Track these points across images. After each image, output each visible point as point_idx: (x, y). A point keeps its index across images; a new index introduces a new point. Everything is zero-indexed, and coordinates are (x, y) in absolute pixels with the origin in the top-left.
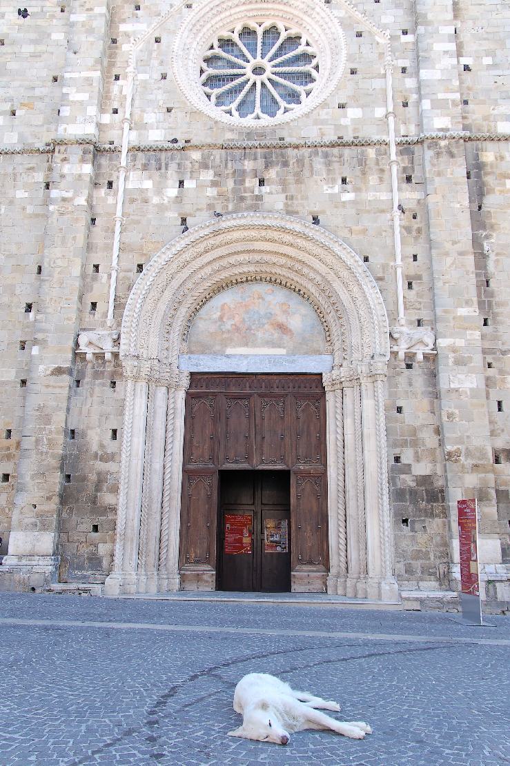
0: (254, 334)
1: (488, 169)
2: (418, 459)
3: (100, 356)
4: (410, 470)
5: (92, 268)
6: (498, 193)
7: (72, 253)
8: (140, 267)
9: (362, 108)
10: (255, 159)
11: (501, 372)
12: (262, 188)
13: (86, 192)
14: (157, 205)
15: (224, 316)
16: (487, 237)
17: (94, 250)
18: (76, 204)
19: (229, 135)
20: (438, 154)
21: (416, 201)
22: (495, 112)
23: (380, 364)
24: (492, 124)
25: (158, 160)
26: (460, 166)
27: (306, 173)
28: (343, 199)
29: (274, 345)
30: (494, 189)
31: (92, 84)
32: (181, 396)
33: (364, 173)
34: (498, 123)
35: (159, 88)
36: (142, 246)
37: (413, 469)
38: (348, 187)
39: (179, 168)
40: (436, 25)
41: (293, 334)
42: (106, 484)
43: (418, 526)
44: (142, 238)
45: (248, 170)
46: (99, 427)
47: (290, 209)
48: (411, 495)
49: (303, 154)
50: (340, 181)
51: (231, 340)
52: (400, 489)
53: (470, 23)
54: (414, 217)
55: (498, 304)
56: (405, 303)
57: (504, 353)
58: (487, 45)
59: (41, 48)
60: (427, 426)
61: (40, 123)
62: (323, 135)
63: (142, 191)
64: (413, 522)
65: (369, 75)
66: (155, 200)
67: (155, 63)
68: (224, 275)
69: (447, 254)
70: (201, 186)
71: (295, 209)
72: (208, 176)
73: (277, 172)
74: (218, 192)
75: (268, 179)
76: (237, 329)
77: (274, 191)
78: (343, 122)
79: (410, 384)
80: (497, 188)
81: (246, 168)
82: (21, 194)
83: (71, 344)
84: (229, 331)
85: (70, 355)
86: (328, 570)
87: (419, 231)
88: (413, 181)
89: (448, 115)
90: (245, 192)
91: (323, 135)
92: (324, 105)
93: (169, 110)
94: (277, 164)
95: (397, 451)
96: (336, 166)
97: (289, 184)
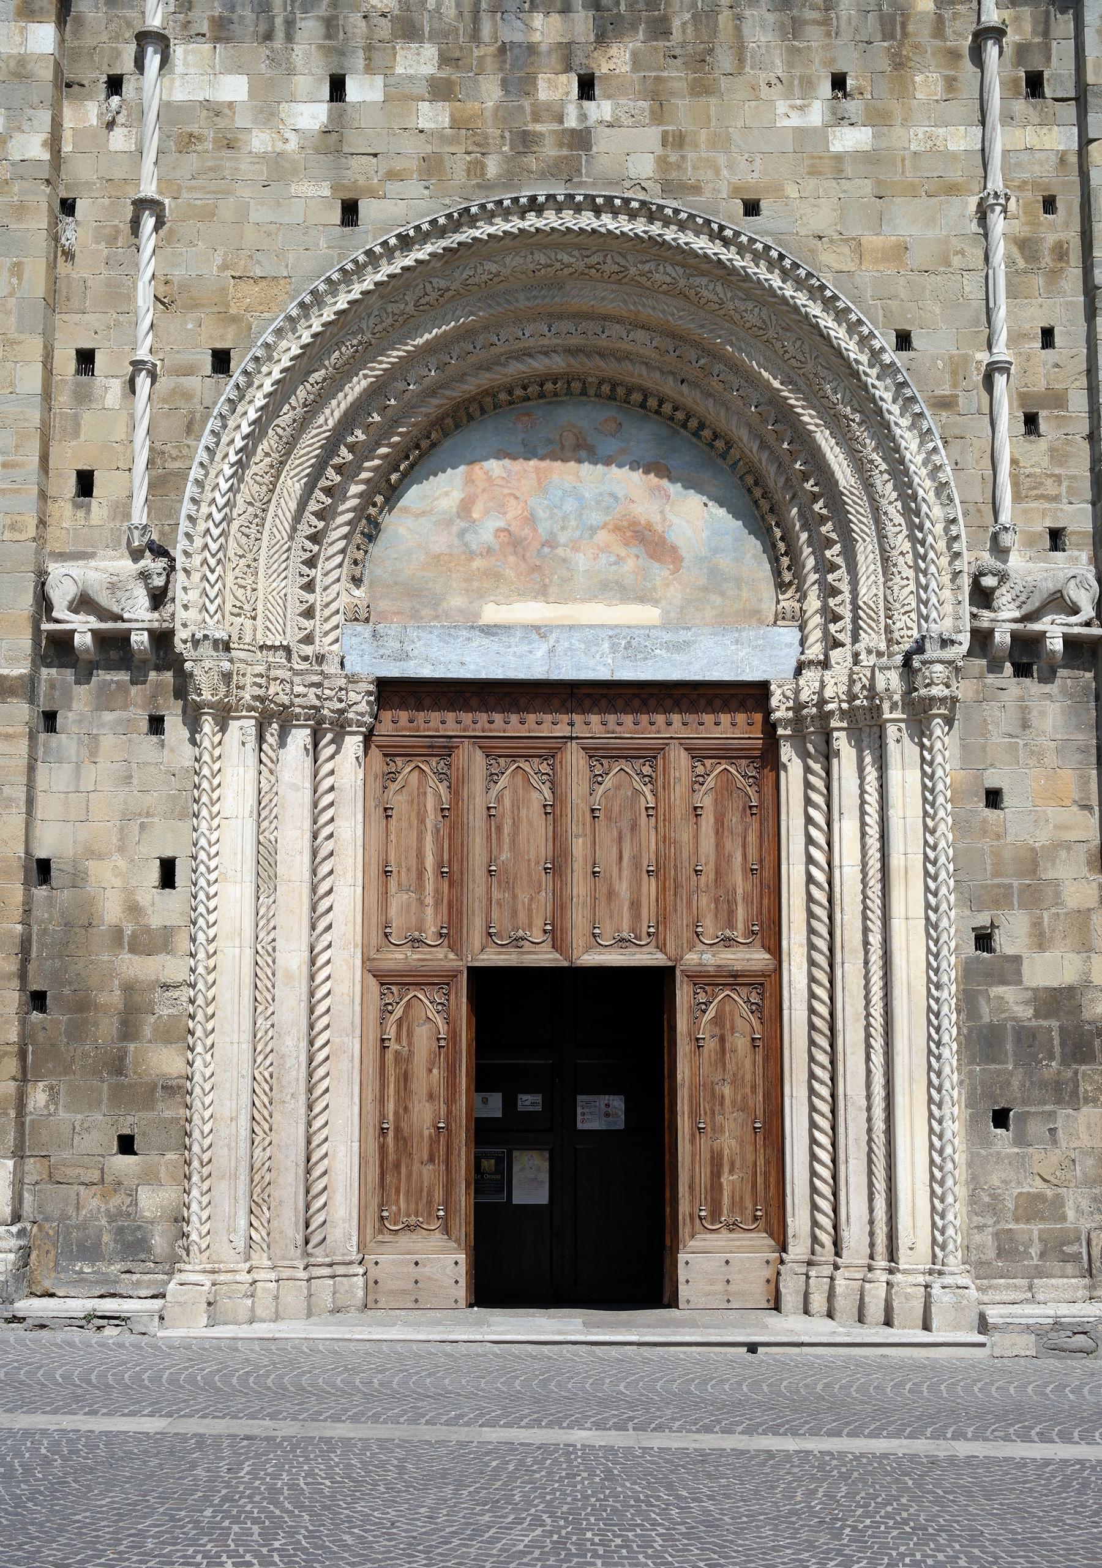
0: (564, 560)
2: (1041, 941)
4: (1019, 973)
5: (66, 362)
7: (13, 319)
8: (221, 361)
13: (45, 117)
14: (263, 157)
15: (473, 503)
17: (75, 303)
18: (17, 157)
21: (1054, 159)
23: (939, 667)
27: (725, 60)
28: (836, 147)
36: (224, 289)
37: (1026, 969)
38: (852, 107)
39: (328, 36)
41: (682, 560)
42: (152, 1019)
43: (1035, 1128)
44: (224, 267)
45: (544, 48)
46: (121, 849)
47: (674, 175)
48: (1018, 1041)
50: (825, 88)
51: (498, 577)
52: (991, 1026)
54: (1049, 205)
56: (1016, 484)
60: (1068, 846)
63: (215, 110)
64: (1023, 1117)
66: (260, 141)
68: (471, 386)
71: (690, 175)
73: (635, 54)
74: (452, 116)
75: (606, 77)
76: (514, 542)
77: (626, 121)
79: (1025, 725)
81: (536, 37)
83: (26, 601)
84: (490, 551)
85: (25, 643)
86: (784, 1248)
87: (1060, 253)
88: (1048, 91)
90: (536, 119)
94: (634, 27)
95: (983, 919)
96: (814, 35)
97: (672, 94)
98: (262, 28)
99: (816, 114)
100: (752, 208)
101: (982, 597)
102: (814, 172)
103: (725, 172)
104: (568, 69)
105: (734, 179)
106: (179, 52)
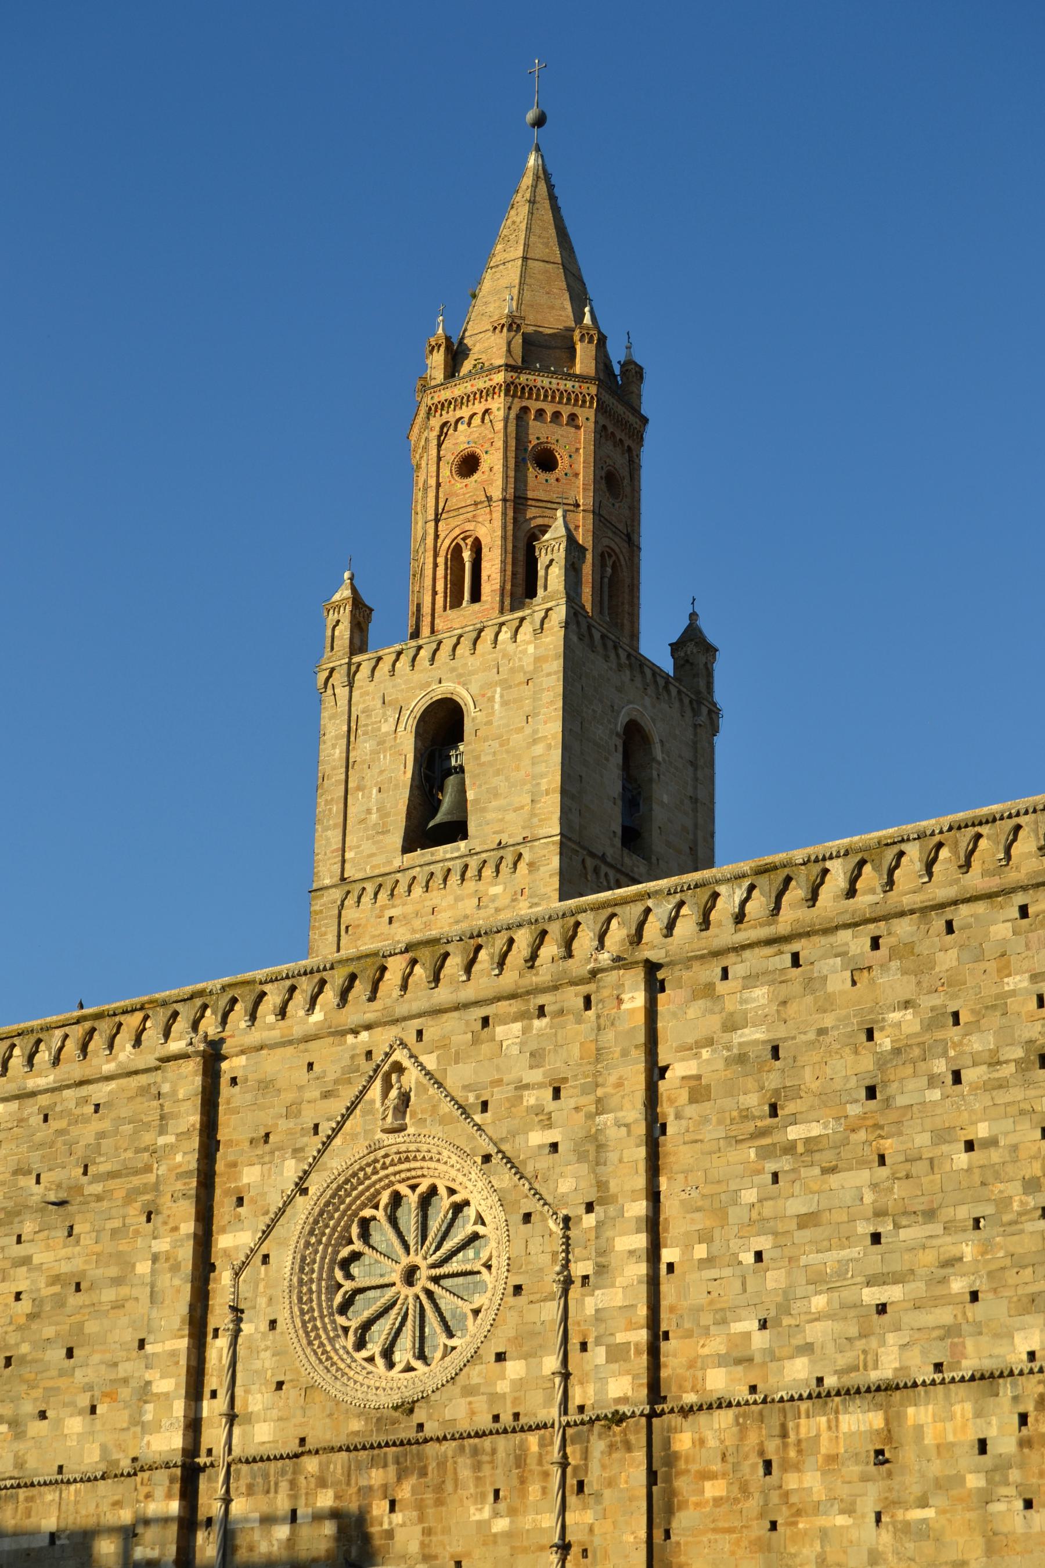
1: (682, 1465)
6: (691, 1507)
9: (525, 1359)
10: (385, 1466)
12: (393, 1516)
19: (356, 1425)
20: (612, 1447)
22: (705, 1351)
24: (700, 1374)
25: (266, 1476)
26: (638, 1466)
27: (449, 1487)
28: (494, 1530)
30: (687, 1501)
31: (177, 1363)
34: (708, 1370)
35: (266, 1350)
38: (502, 1506)
39: (291, 1489)
40: (620, 1201)
45: (376, 1487)
47: (427, 1551)
49: (445, 1451)
53: (681, 1177)
58: (700, 1221)
59: (124, 1291)
61: (125, 1425)
62: (473, 1413)
65: (537, 1297)
67: (262, 1301)
71: (434, 1551)
73: (413, 1487)
75: (401, 1500)
77: (408, 1523)
78: (503, 1387)
80: (693, 1499)
81: (373, 1482)
89: (628, 1373)
91: (473, 1413)
92: (475, 1357)
93: (280, 1385)
94: (413, 1473)
96: (486, 1470)
98: (266, 1488)
99: (486, 1513)
102: (485, 1544)
103: (448, 1547)
104: (385, 1497)
105: (451, 1550)
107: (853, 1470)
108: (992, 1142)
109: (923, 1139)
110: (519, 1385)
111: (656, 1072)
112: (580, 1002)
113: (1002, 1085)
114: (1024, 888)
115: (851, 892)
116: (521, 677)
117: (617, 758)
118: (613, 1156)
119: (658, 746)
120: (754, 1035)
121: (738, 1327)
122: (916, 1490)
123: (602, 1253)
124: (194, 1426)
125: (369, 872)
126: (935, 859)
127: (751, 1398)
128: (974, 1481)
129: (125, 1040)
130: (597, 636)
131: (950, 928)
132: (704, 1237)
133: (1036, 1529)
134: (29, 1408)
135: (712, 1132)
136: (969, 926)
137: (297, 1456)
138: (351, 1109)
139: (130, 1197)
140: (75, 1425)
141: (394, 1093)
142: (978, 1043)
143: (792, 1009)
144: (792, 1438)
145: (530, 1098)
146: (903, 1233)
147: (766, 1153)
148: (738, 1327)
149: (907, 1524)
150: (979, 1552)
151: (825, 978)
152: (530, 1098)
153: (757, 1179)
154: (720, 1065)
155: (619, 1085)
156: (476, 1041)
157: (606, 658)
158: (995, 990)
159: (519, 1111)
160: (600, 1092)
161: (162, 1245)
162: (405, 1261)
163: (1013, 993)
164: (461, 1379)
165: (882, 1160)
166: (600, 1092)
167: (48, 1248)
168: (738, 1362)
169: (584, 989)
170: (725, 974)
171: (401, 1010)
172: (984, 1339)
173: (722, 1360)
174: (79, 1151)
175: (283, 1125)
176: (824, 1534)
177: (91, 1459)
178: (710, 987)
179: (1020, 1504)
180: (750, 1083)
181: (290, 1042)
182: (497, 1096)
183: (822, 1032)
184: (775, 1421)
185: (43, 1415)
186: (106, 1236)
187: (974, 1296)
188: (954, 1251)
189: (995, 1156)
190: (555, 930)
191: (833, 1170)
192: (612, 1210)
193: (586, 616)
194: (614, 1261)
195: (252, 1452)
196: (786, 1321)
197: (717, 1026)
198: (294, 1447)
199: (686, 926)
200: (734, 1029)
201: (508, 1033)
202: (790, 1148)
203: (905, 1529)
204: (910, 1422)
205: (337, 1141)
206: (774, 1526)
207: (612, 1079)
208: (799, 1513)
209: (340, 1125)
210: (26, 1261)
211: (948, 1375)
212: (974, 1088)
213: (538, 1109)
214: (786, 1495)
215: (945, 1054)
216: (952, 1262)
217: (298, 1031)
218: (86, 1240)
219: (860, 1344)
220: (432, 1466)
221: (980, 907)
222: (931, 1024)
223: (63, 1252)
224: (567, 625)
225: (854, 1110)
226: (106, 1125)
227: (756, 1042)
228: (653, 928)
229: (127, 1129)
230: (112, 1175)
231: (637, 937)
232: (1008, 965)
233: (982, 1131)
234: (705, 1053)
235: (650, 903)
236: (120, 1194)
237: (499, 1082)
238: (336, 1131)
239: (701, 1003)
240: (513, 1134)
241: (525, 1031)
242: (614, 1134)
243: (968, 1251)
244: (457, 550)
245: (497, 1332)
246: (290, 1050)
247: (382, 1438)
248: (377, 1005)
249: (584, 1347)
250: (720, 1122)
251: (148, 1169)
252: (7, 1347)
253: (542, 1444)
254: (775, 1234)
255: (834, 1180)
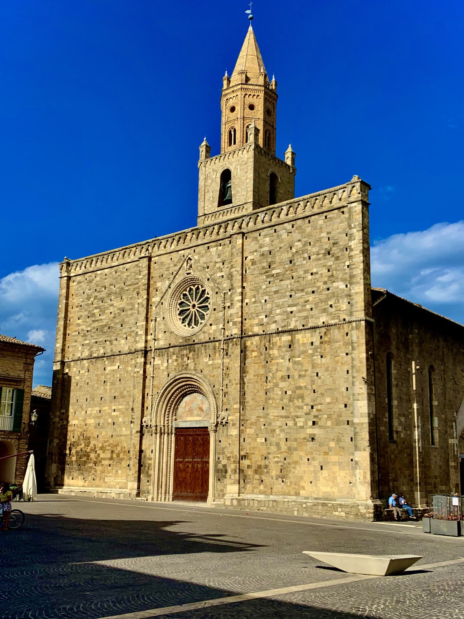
1: (248, 348)
2: (223, 459)
3: (147, 426)
11: (246, 428)
16: (246, 376)
19: (181, 341)
20: (233, 344)
25: (162, 352)
27: (200, 354)
29: (199, 416)
32: (173, 435)
33: (215, 352)
38: (211, 358)
43: (222, 481)
55: (247, 402)
57: (247, 420)
58: (254, 293)
59: (133, 311)
63: (158, 365)
67: (161, 313)
69: (233, 385)
70: (173, 362)
72: (174, 357)
76: (189, 410)
78: (211, 331)
82: (130, 369)
83: (140, 423)
85: (139, 427)
92: (205, 325)
93: (165, 332)
96: (208, 350)
99: (207, 360)
100: (202, 372)
101: (217, 418)
106: (156, 359)
107: (284, 349)
108: (317, 273)
109: (301, 273)
110: (215, 331)
111: (244, 258)
112: (229, 242)
113: (319, 259)
114: (326, 212)
115: (287, 215)
116: (244, 163)
117: (269, 182)
118: (234, 278)
119: (279, 179)
120: (266, 249)
121: (261, 317)
122: (298, 354)
123: (232, 301)
124: (146, 341)
125: (210, 212)
126: (306, 206)
127: (263, 333)
128: (310, 352)
129: (132, 253)
130: (263, 152)
131: (309, 222)
132: (254, 296)
133: (323, 362)
134: (113, 338)
135: (257, 272)
136: (313, 221)
137: (169, 348)
138: (180, 269)
139: (133, 291)
140: (123, 341)
141: (189, 265)
142: (314, 250)
143: (274, 243)
144: (271, 342)
145: (218, 265)
146: (297, 295)
147: (268, 277)
148: (261, 317)
149: (295, 361)
150: (311, 368)
151: (281, 235)
152: (218, 265)
153: (266, 283)
154: (258, 256)
155: (236, 262)
156: (206, 252)
157: (266, 158)
158: (319, 237)
159: (215, 268)
160: (232, 263)
161: (140, 301)
162: (192, 303)
163: (323, 237)
164: (203, 330)
165: (293, 278)
166: (232, 263)
167: (117, 302)
168: (261, 325)
169: (229, 239)
170: (260, 235)
171: (191, 246)
172: (313, 319)
173: (258, 325)
174: (123, 280)
175: (166, 273)
176: (278, 364)
177: (126, 349)
178: (256, 238)
179: (320, 357)
180: (265, 260)
181: (167, 254)
182: (211, 265)
183: (280, 248)
184: (268, 338)
185: (116, 340)
186: (129, 299)
187: (312, 309)
188: (307, 299)
189: (317, 276)
190: (223, 225)
191: (282, 280)
192: (234, 291)
193: (260, 147)
194: (234, 302)
195: (159, 347)
196: (271, 315)
197: (258, 247)
198: (168, 346)
199: (251, 224)
200: (261, 248)
201: (213, 250)
202: (273, 276)
203: (295, 363)
204: (297, 338)
205: (177, 276)
206: (267, 362)
207: (235, 260)
208: (272, 359)
209: (177, 273)
210: (112, 305)
211: (305, 327)
212: (313, 260)
213: (219, 268)
214: (270, 355)
215: (307, 252)
216: (307, 301)
217: (168, 252)
218: (125, 300)
219: (287, 321)
220: (196, 349)
221: (316, 217)
222: (304, 245)
223: (120, 303)
224: (254, 150)
225: (287, 266)
226: (128, 274)
227: (266, 251)
228: (244, 225)
229: (133, 274)
230: (130, 285)
231: (240, 227)
232: (322, 230)
233: (315, 270)
234: (255, 254)
235: (244, 218)
236: (132, 289)
237: (211, 262)
238: (177, 274)
239: (254, 242)
240: (214, 273)
241: (217, 249)
242: (234, 273)
243: (311, 299)
244: (230, 132)
245: (210, 319)
246: (167, 255)
247: (186, 344)
248: (185, 244)
249: (228, 322)
250: (258, 270)
251: (137, 283)
252: (109, 325)
253: (220, 344)
254: (269, 296)
255: (282, 283)
